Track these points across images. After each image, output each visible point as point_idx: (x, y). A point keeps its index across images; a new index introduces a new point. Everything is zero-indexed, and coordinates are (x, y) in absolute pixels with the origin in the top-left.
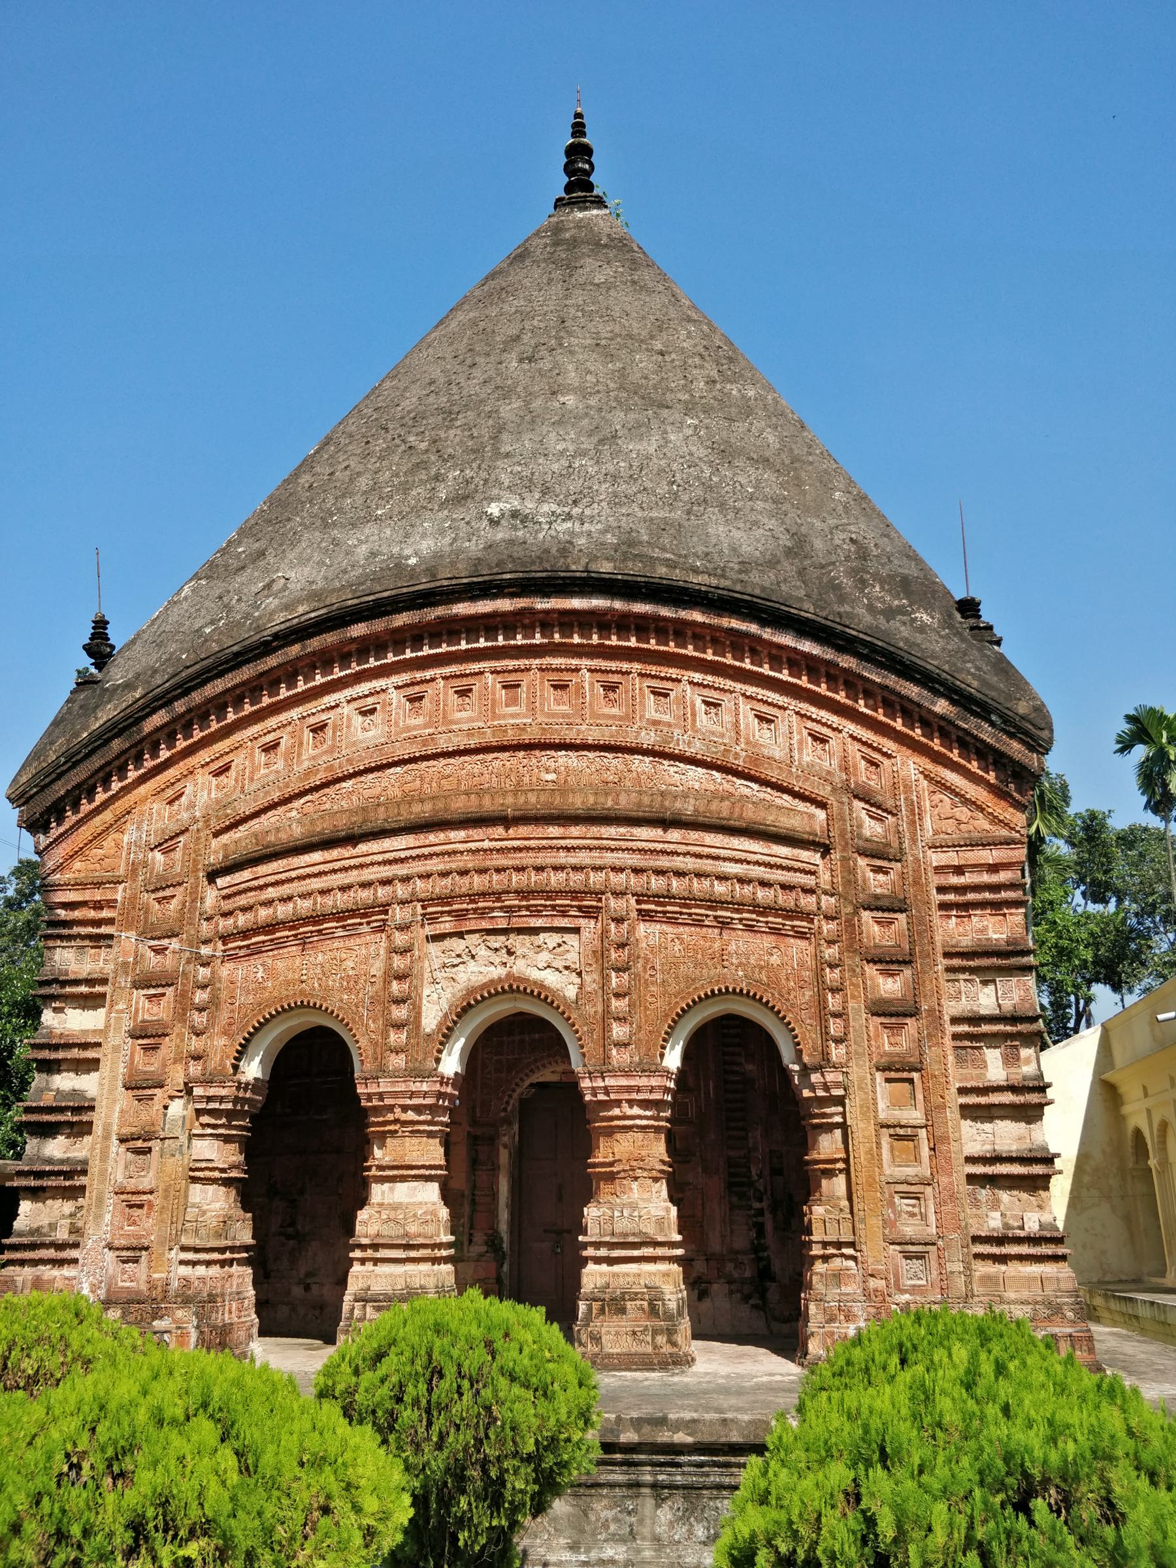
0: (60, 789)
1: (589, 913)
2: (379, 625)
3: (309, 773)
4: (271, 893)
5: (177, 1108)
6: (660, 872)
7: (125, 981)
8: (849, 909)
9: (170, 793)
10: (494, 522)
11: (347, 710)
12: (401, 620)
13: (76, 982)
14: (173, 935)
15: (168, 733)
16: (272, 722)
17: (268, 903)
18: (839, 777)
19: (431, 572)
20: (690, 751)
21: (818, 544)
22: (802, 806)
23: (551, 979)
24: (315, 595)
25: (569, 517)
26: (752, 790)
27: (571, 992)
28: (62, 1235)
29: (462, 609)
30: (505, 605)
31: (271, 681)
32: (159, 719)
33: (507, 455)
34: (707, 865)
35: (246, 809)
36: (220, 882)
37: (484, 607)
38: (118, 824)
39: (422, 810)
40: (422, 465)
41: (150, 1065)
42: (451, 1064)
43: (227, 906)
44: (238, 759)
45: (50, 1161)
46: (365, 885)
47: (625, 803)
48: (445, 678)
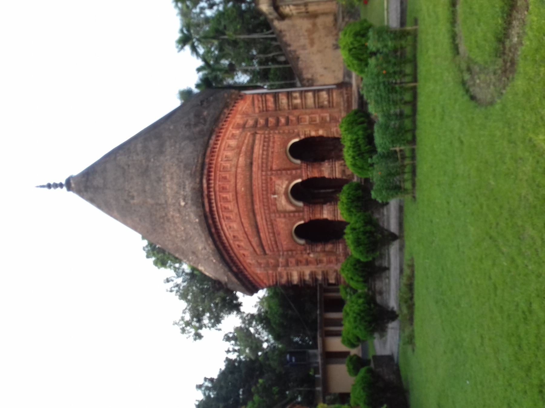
0: (250, 286)
1: (271, 179)
2: (212, 226)
3: (244, 237)
4: (269, 242)
5: (312, 255)
6: (262, 167)
7: (288, 268)
8: (268, 129)
9: (249, 265)
10: (186, 204)
11: (230, 230)
12: (210, 221)
13: (288, 278)
14: (278, 261)
15: (237, 266)
16: (233, 246)
17: (271, 243)
18: (241, 130)
19: (200, 217)
20: (236, 161)
21: (187, 134)
22: (247, 138)
23: (284, 186)
24: (207, 240)
25: (184, 188)
26: (244, 148)
27: (287, 182)
28: (335, 274)
29: (207, 209)
30: (206, 201)
31: (224, 247)
32: (234, 269)
33: (166, 202)
34: (260, 157)
35: (251, 249)
36: (267, 252)
37: (207, 205)
38: (256, 274)
39: (251, 215)
40: (168, 220)
41: (304, 261)
42: (300, 204)
43: (272, 250)
44: (242, 252)
45: (322, 279)
46: (267, 224)
47: (248, 173)
48: (222, 211)
